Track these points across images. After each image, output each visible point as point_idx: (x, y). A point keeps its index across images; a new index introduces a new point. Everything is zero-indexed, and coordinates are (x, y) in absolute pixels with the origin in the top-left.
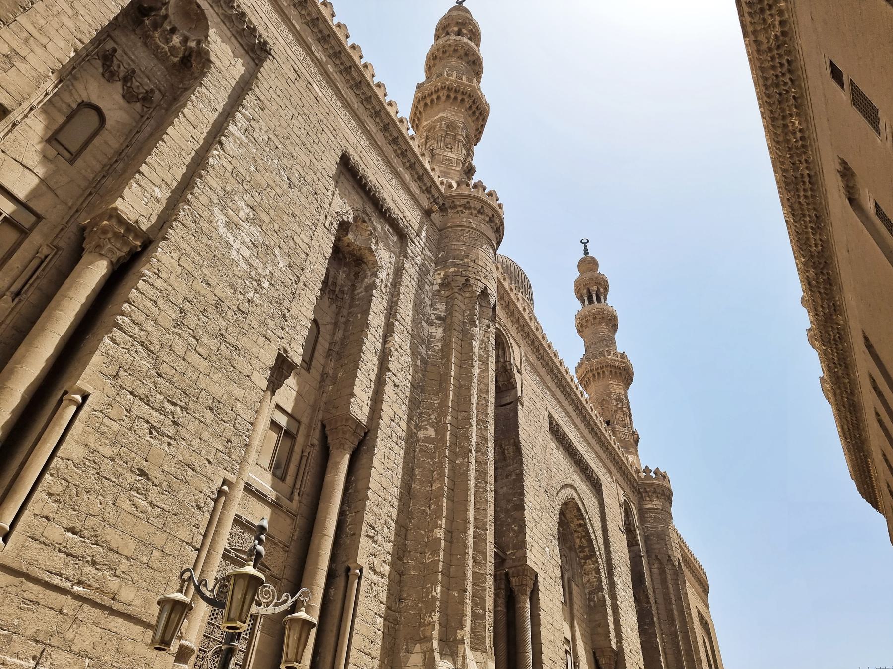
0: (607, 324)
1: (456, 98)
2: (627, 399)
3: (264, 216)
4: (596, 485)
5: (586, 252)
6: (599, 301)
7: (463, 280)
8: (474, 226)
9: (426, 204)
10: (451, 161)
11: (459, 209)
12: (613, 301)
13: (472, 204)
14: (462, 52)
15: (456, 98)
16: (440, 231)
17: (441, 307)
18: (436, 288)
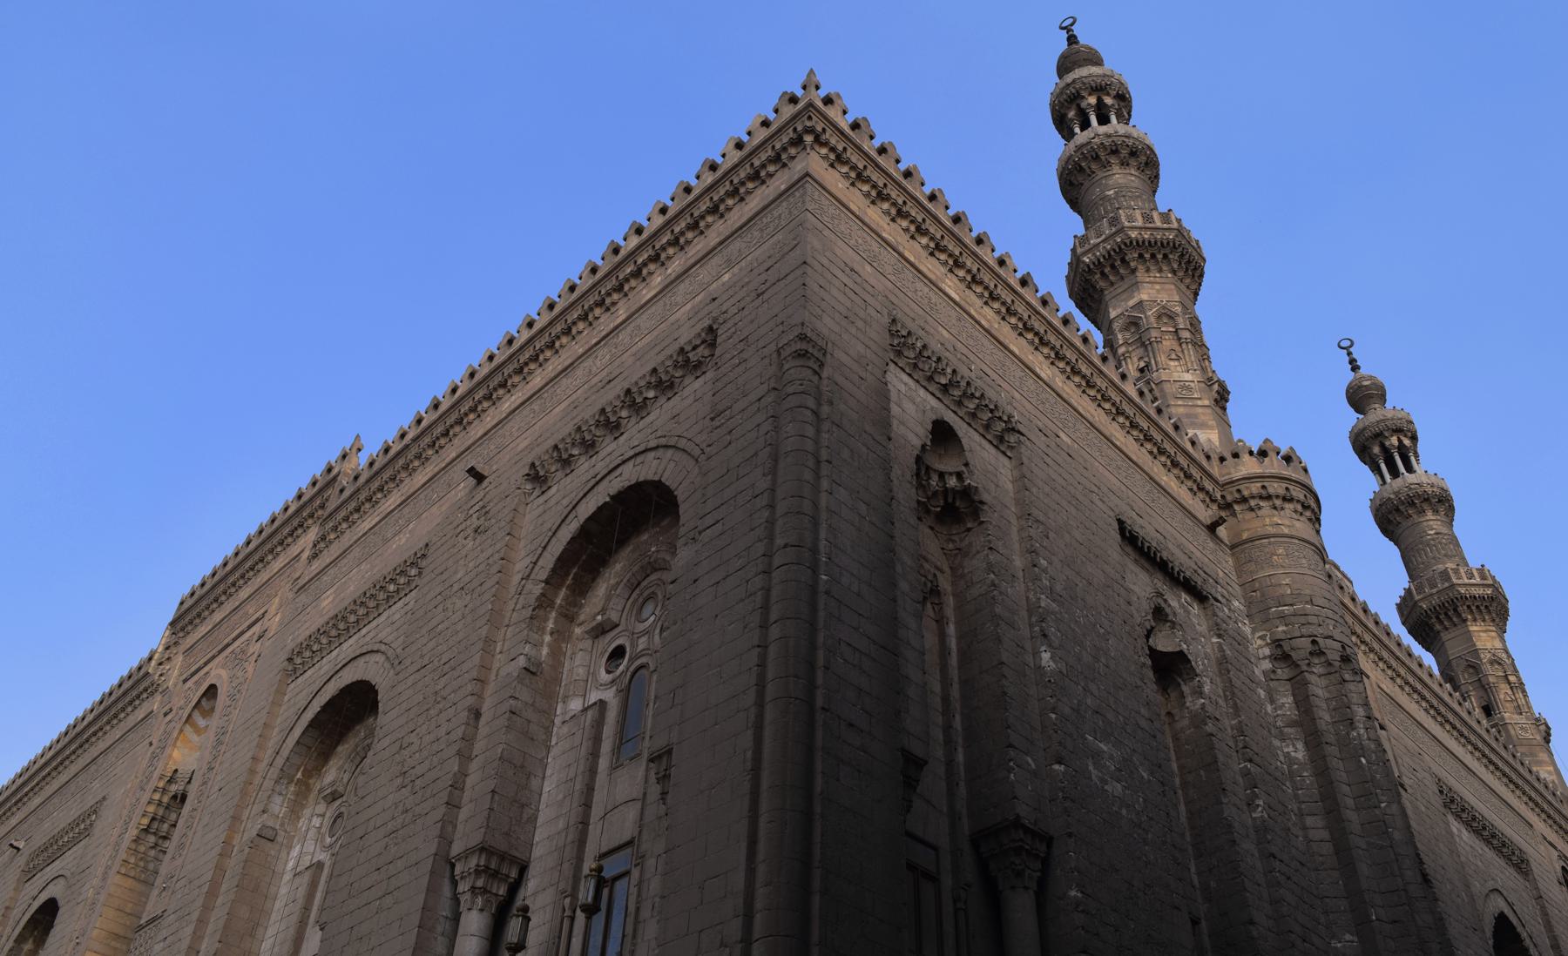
0: (1436, 512)
1: (1153, 256)
2: (1509, 656)
3: (1110, 716)
4: (1521, 865)
5: (1355, 368)
6: (1410, 469)
7: (1305, 643)
8: (1286, 531)
9: (1206, 514)
10: (1189, 389)
11: (1253, 503)
12: (1435, 462)
13: (1271, 491)
14: (1124, 152)
15: (1153, 256)
16: (1232, 547)
17: (1287, 700)
18: (1267, 665)
